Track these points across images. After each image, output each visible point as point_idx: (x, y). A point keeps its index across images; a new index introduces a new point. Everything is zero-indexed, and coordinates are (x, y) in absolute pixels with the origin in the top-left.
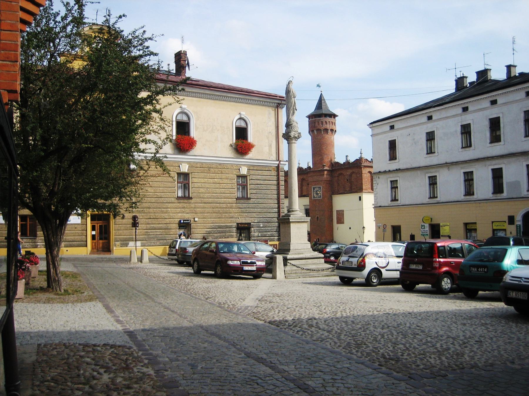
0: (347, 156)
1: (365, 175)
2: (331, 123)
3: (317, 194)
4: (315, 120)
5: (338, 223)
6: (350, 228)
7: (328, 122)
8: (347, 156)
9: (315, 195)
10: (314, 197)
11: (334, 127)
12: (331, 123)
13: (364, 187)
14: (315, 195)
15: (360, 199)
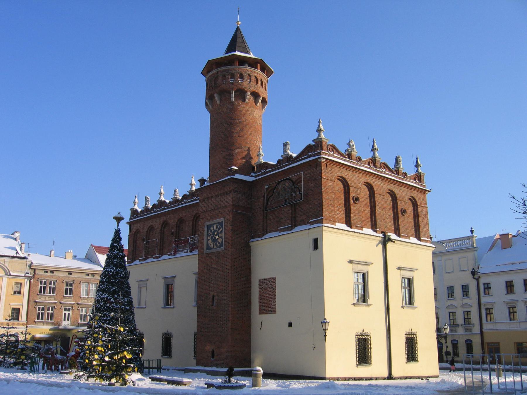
0: (285, 145)
1: (330, 184)
2: (253, 78)
3: (215, 240)
4: (218, 72)
5: (261, 312)
6: (290, 325)
7: (245, 76)
8: (285, 145)
9: (210, 242)
10: (208, 248)
11: (262, 90)
12: (253, 78)
13: (326, 214)
14: (210, 242)
15: (316, 244)
